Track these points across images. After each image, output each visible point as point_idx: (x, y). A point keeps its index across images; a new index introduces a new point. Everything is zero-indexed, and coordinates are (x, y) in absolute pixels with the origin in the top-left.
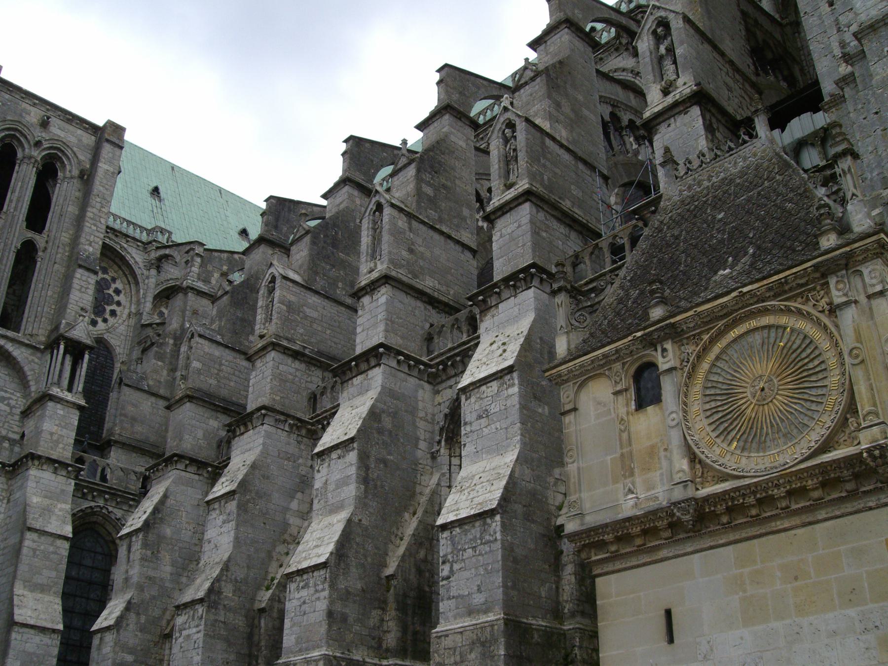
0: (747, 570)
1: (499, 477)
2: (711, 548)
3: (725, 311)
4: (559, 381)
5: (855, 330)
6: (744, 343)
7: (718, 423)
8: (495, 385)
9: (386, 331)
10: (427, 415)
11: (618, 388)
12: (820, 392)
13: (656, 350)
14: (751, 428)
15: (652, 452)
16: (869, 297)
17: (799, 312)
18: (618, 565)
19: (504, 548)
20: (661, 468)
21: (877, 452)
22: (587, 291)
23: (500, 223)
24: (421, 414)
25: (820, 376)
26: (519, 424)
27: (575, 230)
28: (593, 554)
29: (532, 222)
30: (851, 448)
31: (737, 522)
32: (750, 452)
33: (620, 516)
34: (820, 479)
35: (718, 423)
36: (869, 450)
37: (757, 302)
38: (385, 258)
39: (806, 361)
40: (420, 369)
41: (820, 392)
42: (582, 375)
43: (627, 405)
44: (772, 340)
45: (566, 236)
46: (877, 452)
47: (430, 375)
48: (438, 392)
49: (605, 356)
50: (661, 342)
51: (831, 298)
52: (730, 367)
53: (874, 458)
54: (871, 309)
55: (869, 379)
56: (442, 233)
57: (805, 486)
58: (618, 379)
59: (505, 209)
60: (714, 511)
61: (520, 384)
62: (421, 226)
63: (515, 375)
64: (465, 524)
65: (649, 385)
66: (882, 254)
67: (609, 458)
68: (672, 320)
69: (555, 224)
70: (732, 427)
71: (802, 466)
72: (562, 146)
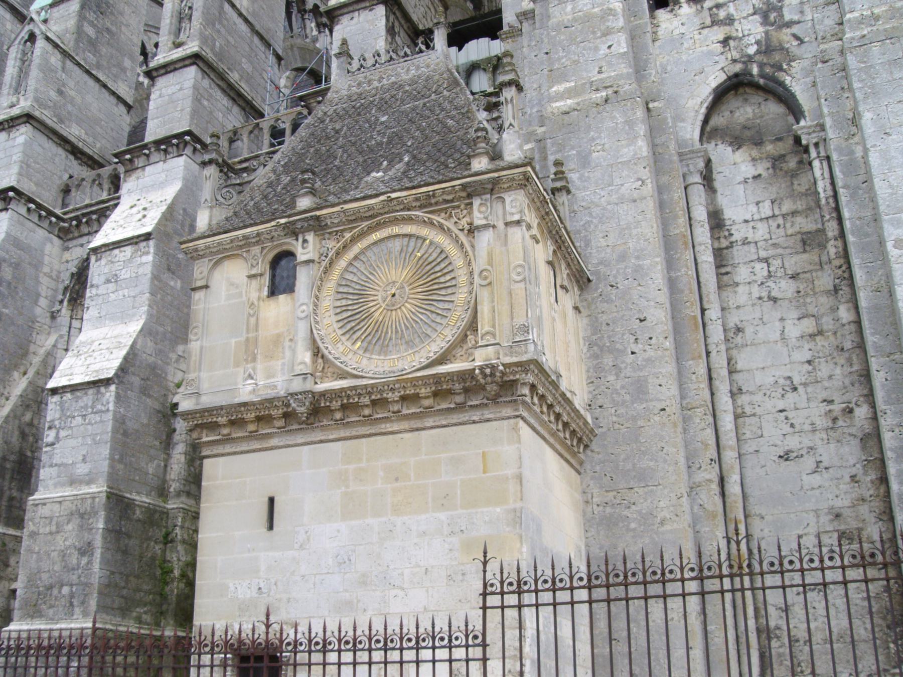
0: (351, 467)
1: (119, 346)
2: (321, 442)
3: (370, 213)
4: (195, 256)
6: (384, 248)
7: (346, 321)
8: (128, 250)
9: (20, 174)
10: (52, 271)
11: (254, 271)
12: (446, 306)
13: (297, 239)
14: (377, 331)
15: (277, 340)
16: (507, 224)
17: (441, 227)
18: (228, 448)
19: (115, 419)
20: (283, 358)
21: (488, 371)
22: (240, 169)
23: (161, 82)
24: (46, 269)
25: (449, 291)
26: (148, 295)
27: (239, 105)
28: (204, 435)
29: (195, 87)
30: (466, 364)
31: (349, 420)
32: (372, 354)
33: (237, 400)
34: (433, 388)
35: (346, 321)
36: (481, 368)
37: (402, 210)
38: (31, 94)
39: (439, 274)
40: (51, 222)
41: (446, 306)
42: (219, 252)
43: (260, 290)
44: (410, 249)
45: (228, 108)
46: (488, 371)
47: (61, 229)
48: (67, 249)
49: (245, 237)
50: (303, 233)
51: (472, 219)
52: (366, 269)
53: (485, 376)
54: (506, 235)
55: (493, 301)
56: (98, 80)
57: (418, 394)
58: (255, 263)
59: (168, 68)
60: (329, 406)
61: (155, 254)
62: (76, 68)
63: (152, 243)
64: (77, 390)
65: (285, 274)
66: (525, 186)
67: (233, 341)
68: (318, 213)
69: (219, 94)
70: (358, 327)
72: (240, 15)
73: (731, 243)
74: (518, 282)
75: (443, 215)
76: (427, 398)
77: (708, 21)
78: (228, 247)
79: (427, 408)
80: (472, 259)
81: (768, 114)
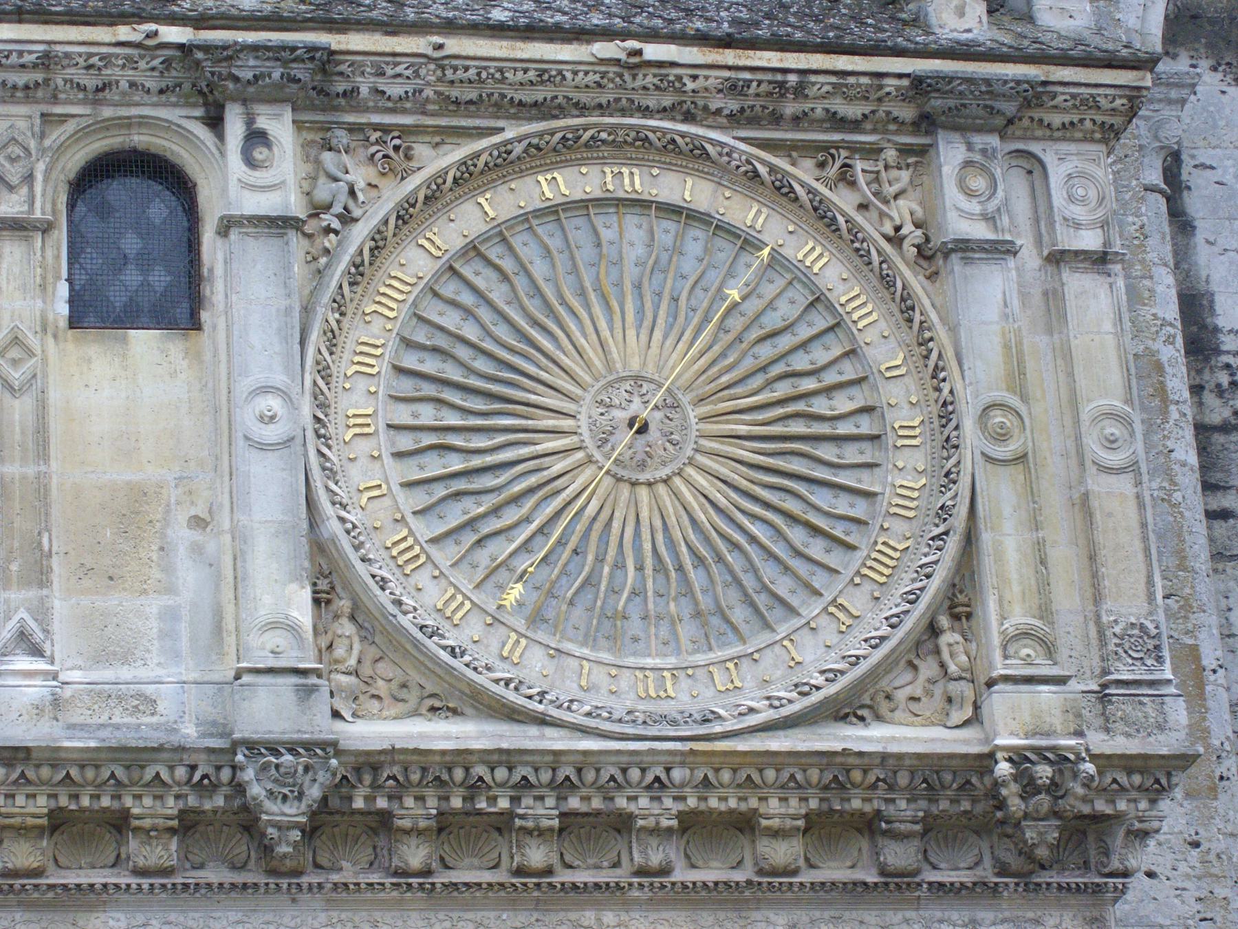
3: (539, 94)
5: (1007, 346)
7: (440, 491)
13: (215, 122)
15: (133, 511)
20: (171, 590)
21: (1044, 772)
25: (851, 454)
34: (814, 804)
35: (440, 491)
36: (1018, 758)
37: (664, 112)
39: (809, 384)
41: (843, 505)
46: (1044, 772)
68: (335, 41)
71: (778, 743)
74: (1109, 470)
75: (809, 163)
76: (775, 834)
79: (774, 873)
80: (950, 353)
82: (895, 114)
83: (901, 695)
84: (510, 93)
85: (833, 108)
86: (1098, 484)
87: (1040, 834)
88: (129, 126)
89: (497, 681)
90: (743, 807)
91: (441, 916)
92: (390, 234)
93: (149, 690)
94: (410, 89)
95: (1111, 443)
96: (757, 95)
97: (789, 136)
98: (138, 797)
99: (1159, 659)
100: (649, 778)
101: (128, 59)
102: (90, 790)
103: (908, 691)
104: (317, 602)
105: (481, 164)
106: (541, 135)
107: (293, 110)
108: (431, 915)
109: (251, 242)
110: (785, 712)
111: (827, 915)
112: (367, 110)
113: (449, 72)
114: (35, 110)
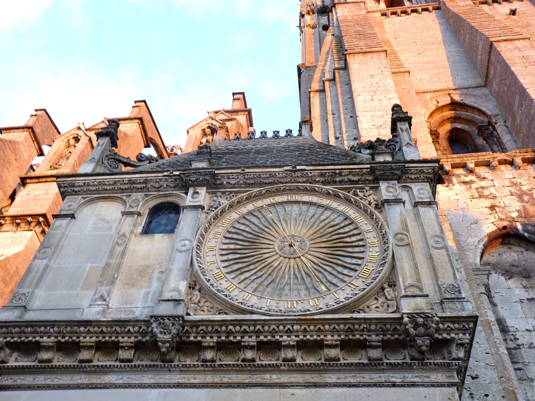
5: (402, 222)
7: (232, 262)
13: (187, 194)
16: (416, 205)
18: (40, 380)
20: (150, 287)
21: (420, 320)
34: (343, 337)
36: (411, 316)
37: (304, 182)
41: (354, 261)
50: (194, 186)
70: (247, 269)
73: (518, 345)
77: (476, 195)
78: (108, 188)
81: (531, 259)
82: (367, 178)
83: (373, 307)
84: (262, 181)
85: (350, 178)
86: (435, 252)
87: (423, 342)
88: (167, 196)
89: (239, 303)
90: (319, 338)
91: (218, 376)
92: (227, 209)
93: (134, 309)
94: (236, 181)
95: (437, 242)
96: (329, 176)
97: (339, 186)
98: (123, 337)
99: (460, 293)
100: (286, 328)
101: (166, 179)
102: (109, 335)
103: (376, 305)
104: (190, 288)
105: (253, 195)
106: (270, 188)
107: (207, 189)
108: (215, 376)
109: (189, 212)
110: (331, 308)
111: (351, 375)
112: (226, 188)
113: (246, 177)
114: (144, 194)
